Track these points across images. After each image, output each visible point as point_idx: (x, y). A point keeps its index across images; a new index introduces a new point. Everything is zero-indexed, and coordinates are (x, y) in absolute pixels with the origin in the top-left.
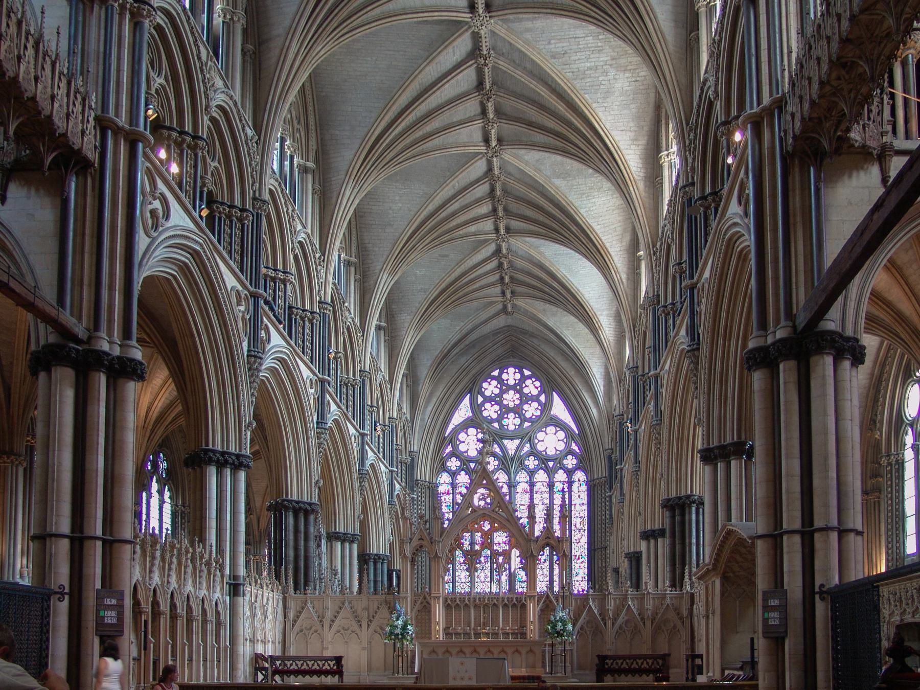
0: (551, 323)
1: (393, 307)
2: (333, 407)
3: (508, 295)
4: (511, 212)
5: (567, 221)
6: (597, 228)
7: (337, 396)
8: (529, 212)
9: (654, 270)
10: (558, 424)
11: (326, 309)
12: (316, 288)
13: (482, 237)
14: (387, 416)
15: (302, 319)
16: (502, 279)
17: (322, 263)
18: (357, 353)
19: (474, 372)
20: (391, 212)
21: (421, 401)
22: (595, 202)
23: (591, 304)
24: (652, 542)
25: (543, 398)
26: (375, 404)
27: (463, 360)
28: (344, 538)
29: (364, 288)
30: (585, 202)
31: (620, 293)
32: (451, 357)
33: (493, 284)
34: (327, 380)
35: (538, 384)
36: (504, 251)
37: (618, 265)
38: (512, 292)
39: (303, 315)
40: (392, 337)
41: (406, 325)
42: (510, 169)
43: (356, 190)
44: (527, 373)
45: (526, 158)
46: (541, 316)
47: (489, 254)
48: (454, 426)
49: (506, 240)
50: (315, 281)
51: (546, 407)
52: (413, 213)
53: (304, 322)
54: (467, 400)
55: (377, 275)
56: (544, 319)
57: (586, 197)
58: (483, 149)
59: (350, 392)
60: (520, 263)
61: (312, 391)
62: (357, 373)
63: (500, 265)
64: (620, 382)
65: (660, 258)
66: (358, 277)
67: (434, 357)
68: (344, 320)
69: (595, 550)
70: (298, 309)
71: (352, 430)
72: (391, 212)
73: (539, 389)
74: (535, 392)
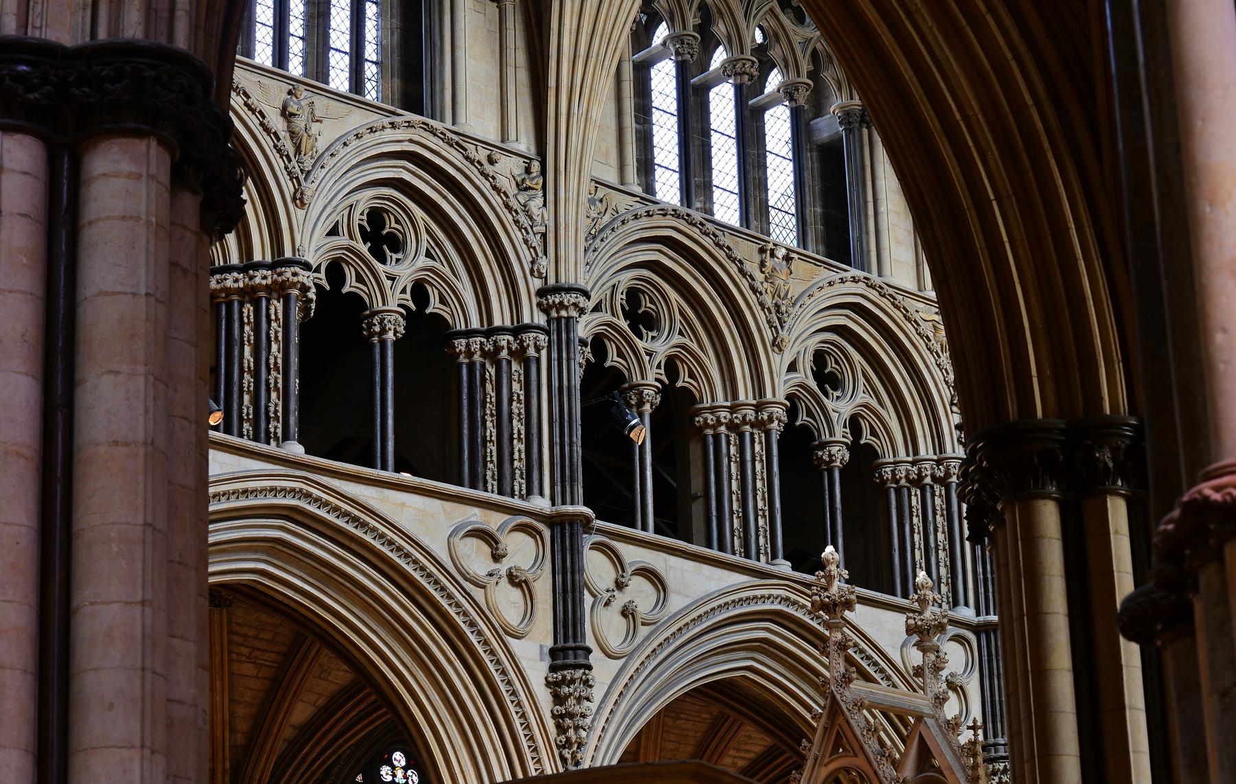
11: (561, 305)
12: (520, 256)
15: (492, 356)
39: (489, 347)
53: (497, 364)
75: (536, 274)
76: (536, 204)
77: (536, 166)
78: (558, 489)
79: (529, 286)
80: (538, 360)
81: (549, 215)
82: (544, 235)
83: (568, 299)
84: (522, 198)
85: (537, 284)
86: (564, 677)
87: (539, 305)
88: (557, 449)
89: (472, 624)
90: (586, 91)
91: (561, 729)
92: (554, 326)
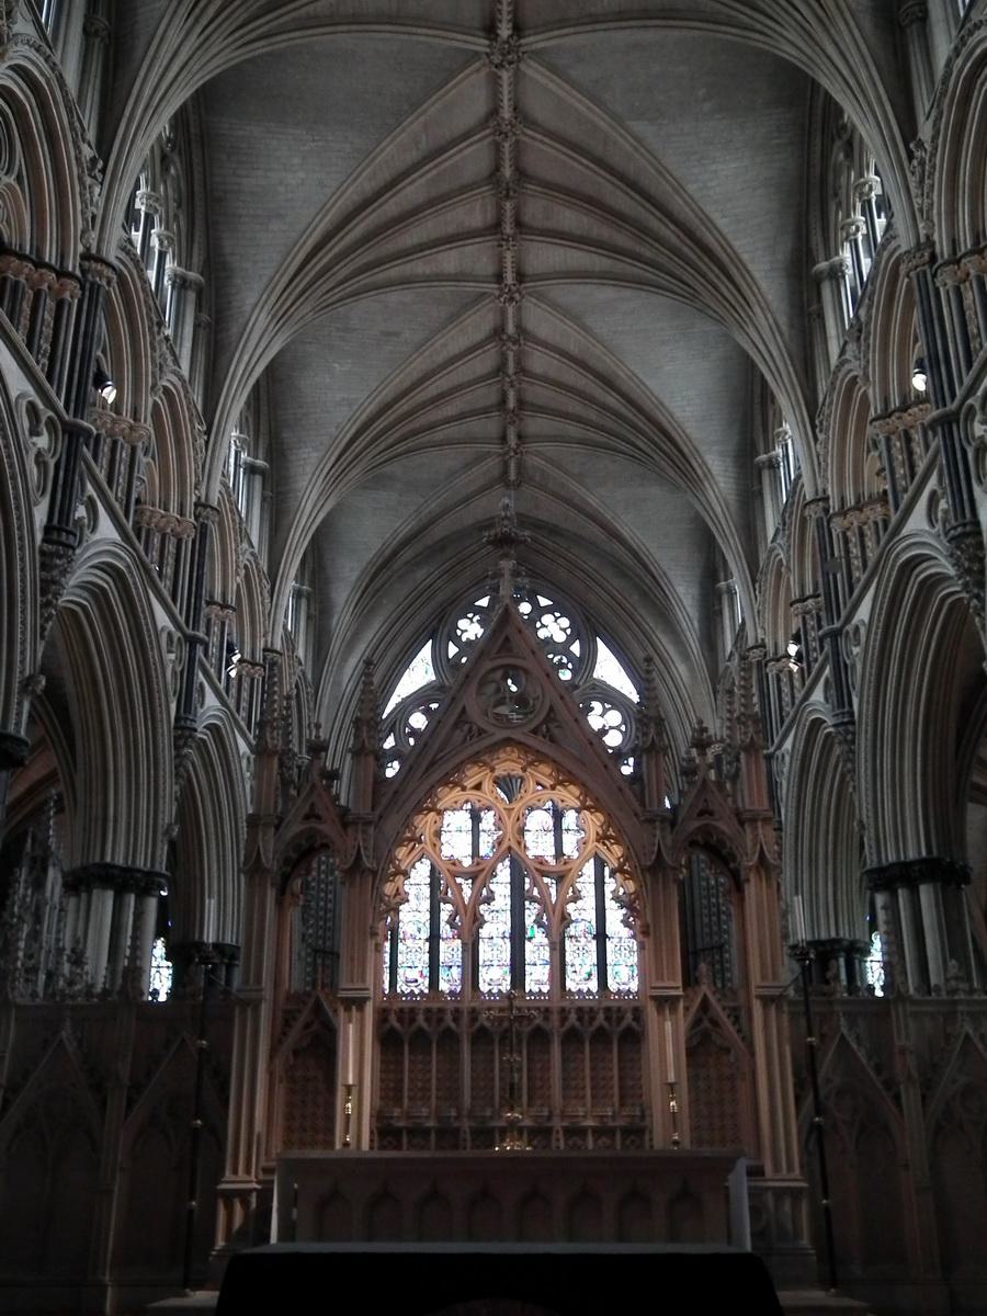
0: (593, 501)
1: (285, 435)
2: (106, 529)
3: (512, 441)
4: (531, 228)
5: (654, 223)
6: (721, 222)
7: (127, 516)
8: (569, 218)
9: (914, 191)
10: (611, 698)
12: (77, 224)
13: (471, 288)
14: (260, 644)
16: (503, 401)
17: (100, 178)
18: (190, 467)
19: (440, 597)
20: (282, 189)
21: (336, 645)
22: (716, 171)
23: (688, 431)
24: (902, 895)
25: (576, 648)
26: (231, 599)
27: (421, 574)
28: (127, 882)
29: (216, 342)
30: (696, 171)
31: (775, 353)
32: (396, 567)
33: (485, 411)
34: (88, 432)
35: (565, 622)
36: (511, 329)
37: (770, 297)
38: (520, 437)
40: (279, 493)
41: (310, 469)
42: (539, 109)
43: (193, 41)
44: (544, 602)
45: (573, 73)
46: (574, 486)
47: (479, 337)
48: (399, 700)
49: (517, 296)
50: (75, 207)
51: (587, 661)
52: (328, 191)
54: (426, 652)
55: (247, 315)
56: (582, 491)
57: (698, 161)
58: (480, 44)
59: (171, 548)
60: (539, 362)
61: (43, 441)
62: (190, 508)
63: (500, 369)
64: (754, 582)
65: (933, 155)
66: (205, 317)
67: (364, 564)
68: (158, 361)
69: (696, 953)
70: (22, 257)
71: (162, 619)
72: (282, 189)
73: (569, 631)
74: (560, 637)
75: (84, 241)
76: (97, 190)
77: (100, 164)
78: (72, 405)
79: (76, 249)
80: (70, 305)
81: (101, 204)
82: (94, 217)
83: (108, 272)
84: (88, 181)
85: (81, 248)
86: (57, 550)
87: (81, 265)
88: (76, 375)
89: (13, 478)
90: (148, 132)
91: (44, 593)
92: (88, 286)
